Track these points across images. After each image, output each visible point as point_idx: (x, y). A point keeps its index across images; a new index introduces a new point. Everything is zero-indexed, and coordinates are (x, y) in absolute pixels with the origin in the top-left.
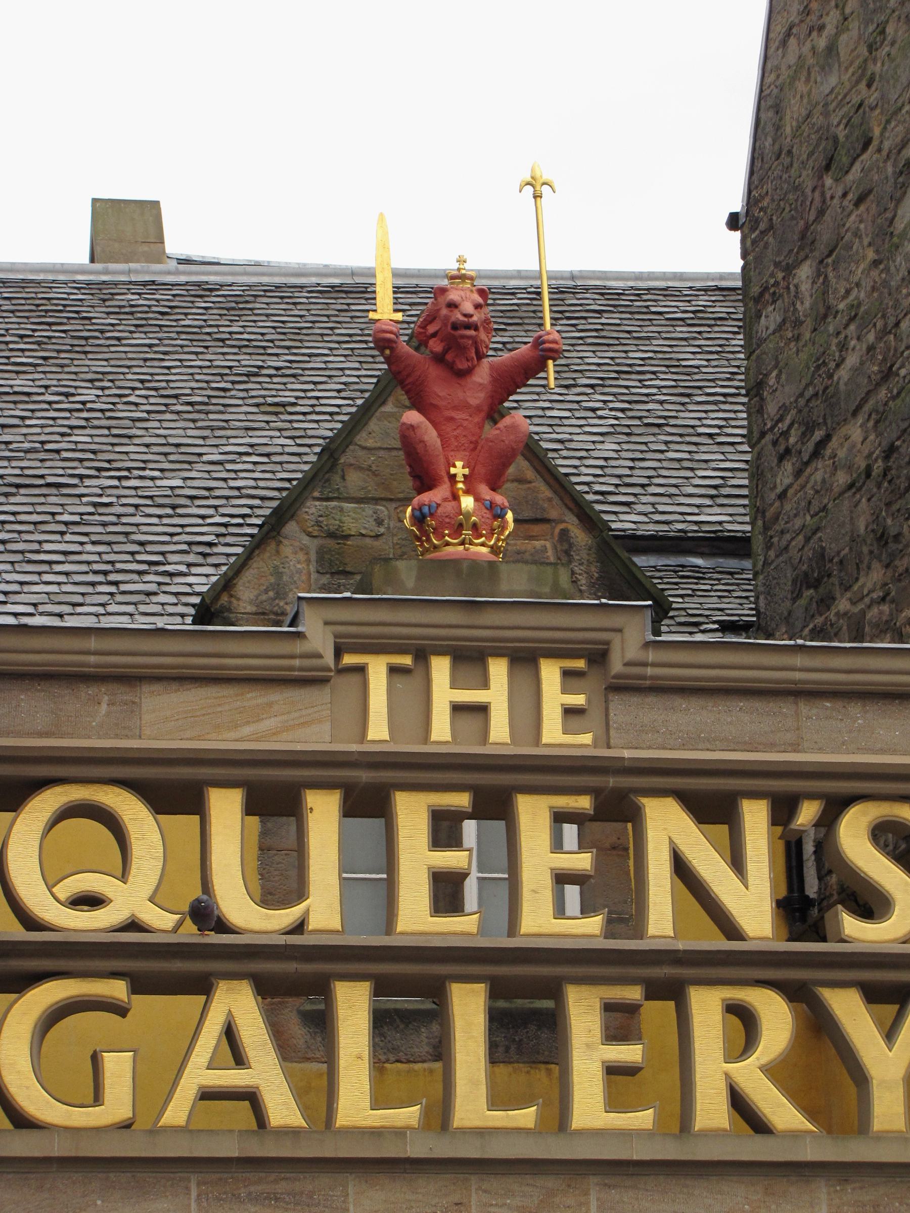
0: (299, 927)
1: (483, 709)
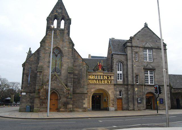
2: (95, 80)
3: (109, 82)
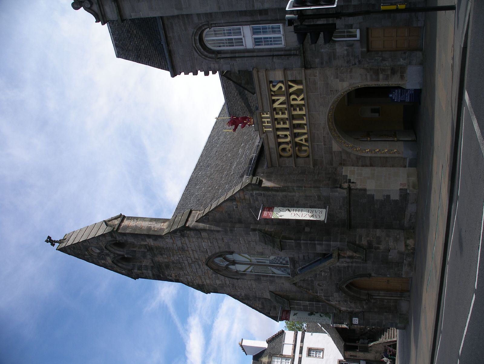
0: (289, 135)
1: (267, 121)
2: (297, 140)
3: (296, 87)
